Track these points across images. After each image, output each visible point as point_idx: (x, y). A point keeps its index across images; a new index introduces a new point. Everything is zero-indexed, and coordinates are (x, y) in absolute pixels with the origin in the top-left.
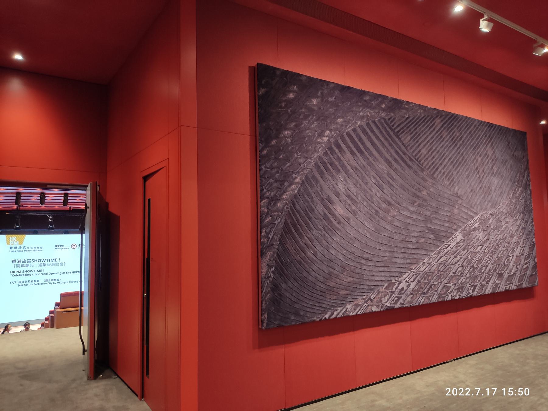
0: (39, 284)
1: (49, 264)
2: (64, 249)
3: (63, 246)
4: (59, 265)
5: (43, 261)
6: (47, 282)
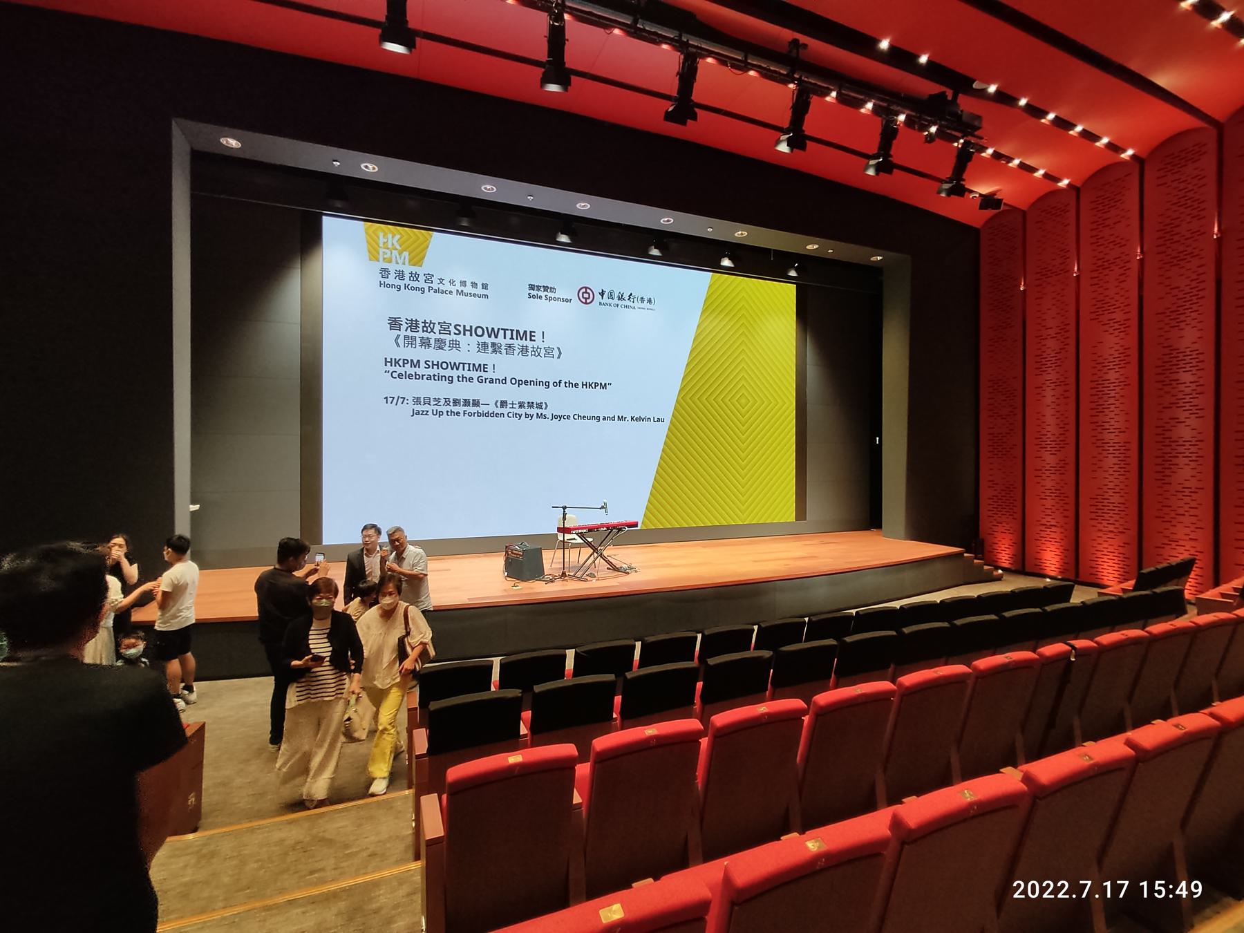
1: (510, 349)
2: (555, 299)
3: (553, 290)
5: (490, 336)
6: (503, 410)
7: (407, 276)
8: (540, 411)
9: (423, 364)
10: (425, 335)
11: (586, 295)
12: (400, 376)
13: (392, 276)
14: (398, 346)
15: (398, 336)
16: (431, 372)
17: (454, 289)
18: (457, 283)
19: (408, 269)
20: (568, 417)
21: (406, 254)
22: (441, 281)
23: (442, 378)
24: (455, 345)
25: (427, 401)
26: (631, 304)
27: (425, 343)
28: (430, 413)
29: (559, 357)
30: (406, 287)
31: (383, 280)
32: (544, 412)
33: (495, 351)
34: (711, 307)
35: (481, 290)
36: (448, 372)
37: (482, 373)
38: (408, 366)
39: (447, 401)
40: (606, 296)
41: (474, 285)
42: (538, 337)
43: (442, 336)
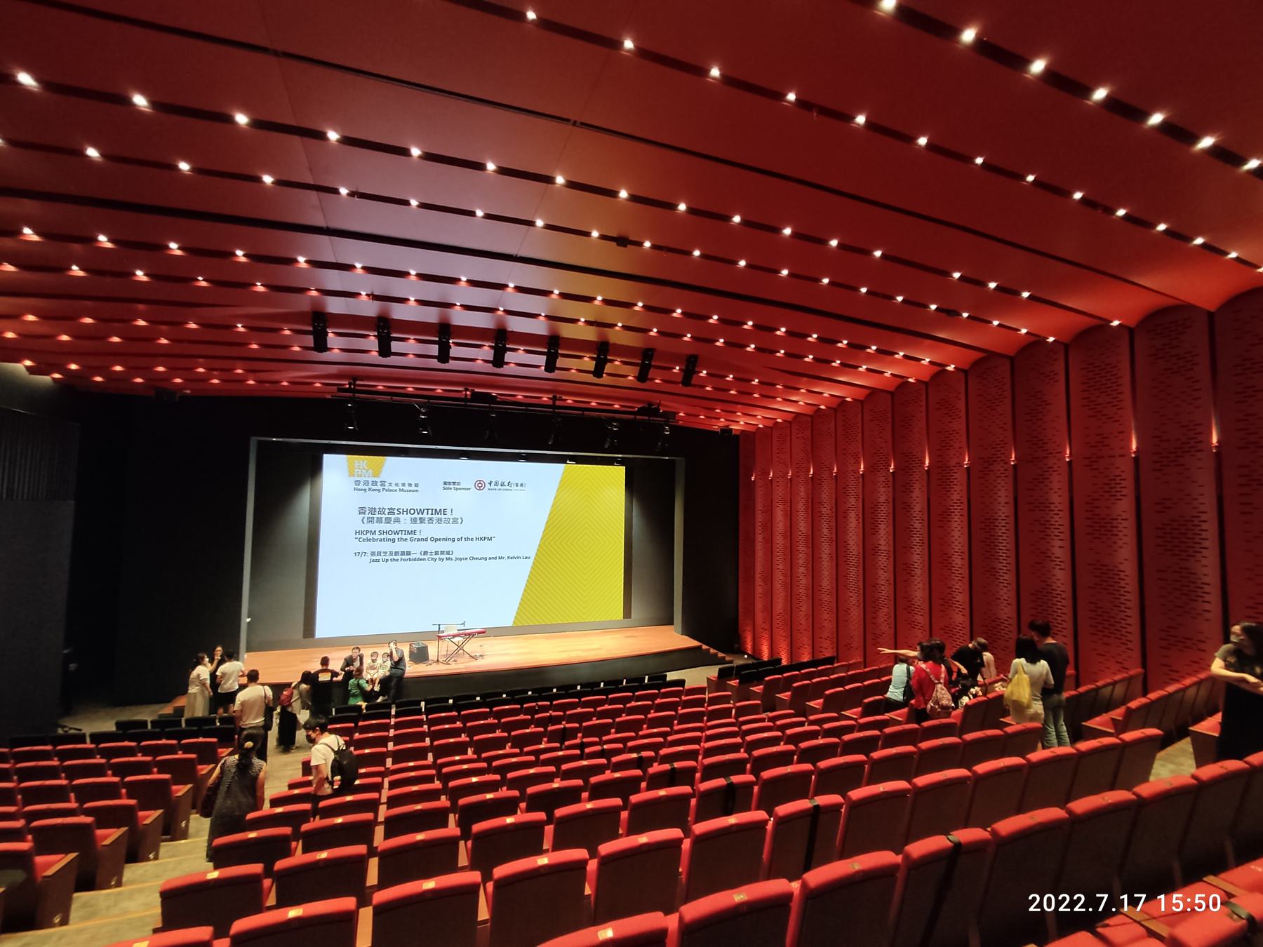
0: (410, 560)
1: (431, 520)
2: (460, 489)
3: (459, 484)
5: (418, 514)
6: (426, 557)
7: (370, 483)
8: (448, 556)
9: (377, 533)
10: (380, 516)
11: (480, 485)
14: (363, 523)
15: (364, 518)
16: (382, 537)
17: (397, 488)
18: (400, 485)
20: (466, 559)
21: (370, 471)
22: (390, 484)
24: (397, 520)
25: (379, 553)
26: (510, 488)
27: (379, 520)
28: (381, 560)
29: (461, 523)
30: (369, 489)
31: (356, 487)
32: (451, 556)
33: (421, 522)
34: (563, 485)
35: (414, 488)
36: (392, 536)
37: (413, 536)
39: (391, 553)
40: (493, 484)
42: (448, 512)
43: (390, 516)
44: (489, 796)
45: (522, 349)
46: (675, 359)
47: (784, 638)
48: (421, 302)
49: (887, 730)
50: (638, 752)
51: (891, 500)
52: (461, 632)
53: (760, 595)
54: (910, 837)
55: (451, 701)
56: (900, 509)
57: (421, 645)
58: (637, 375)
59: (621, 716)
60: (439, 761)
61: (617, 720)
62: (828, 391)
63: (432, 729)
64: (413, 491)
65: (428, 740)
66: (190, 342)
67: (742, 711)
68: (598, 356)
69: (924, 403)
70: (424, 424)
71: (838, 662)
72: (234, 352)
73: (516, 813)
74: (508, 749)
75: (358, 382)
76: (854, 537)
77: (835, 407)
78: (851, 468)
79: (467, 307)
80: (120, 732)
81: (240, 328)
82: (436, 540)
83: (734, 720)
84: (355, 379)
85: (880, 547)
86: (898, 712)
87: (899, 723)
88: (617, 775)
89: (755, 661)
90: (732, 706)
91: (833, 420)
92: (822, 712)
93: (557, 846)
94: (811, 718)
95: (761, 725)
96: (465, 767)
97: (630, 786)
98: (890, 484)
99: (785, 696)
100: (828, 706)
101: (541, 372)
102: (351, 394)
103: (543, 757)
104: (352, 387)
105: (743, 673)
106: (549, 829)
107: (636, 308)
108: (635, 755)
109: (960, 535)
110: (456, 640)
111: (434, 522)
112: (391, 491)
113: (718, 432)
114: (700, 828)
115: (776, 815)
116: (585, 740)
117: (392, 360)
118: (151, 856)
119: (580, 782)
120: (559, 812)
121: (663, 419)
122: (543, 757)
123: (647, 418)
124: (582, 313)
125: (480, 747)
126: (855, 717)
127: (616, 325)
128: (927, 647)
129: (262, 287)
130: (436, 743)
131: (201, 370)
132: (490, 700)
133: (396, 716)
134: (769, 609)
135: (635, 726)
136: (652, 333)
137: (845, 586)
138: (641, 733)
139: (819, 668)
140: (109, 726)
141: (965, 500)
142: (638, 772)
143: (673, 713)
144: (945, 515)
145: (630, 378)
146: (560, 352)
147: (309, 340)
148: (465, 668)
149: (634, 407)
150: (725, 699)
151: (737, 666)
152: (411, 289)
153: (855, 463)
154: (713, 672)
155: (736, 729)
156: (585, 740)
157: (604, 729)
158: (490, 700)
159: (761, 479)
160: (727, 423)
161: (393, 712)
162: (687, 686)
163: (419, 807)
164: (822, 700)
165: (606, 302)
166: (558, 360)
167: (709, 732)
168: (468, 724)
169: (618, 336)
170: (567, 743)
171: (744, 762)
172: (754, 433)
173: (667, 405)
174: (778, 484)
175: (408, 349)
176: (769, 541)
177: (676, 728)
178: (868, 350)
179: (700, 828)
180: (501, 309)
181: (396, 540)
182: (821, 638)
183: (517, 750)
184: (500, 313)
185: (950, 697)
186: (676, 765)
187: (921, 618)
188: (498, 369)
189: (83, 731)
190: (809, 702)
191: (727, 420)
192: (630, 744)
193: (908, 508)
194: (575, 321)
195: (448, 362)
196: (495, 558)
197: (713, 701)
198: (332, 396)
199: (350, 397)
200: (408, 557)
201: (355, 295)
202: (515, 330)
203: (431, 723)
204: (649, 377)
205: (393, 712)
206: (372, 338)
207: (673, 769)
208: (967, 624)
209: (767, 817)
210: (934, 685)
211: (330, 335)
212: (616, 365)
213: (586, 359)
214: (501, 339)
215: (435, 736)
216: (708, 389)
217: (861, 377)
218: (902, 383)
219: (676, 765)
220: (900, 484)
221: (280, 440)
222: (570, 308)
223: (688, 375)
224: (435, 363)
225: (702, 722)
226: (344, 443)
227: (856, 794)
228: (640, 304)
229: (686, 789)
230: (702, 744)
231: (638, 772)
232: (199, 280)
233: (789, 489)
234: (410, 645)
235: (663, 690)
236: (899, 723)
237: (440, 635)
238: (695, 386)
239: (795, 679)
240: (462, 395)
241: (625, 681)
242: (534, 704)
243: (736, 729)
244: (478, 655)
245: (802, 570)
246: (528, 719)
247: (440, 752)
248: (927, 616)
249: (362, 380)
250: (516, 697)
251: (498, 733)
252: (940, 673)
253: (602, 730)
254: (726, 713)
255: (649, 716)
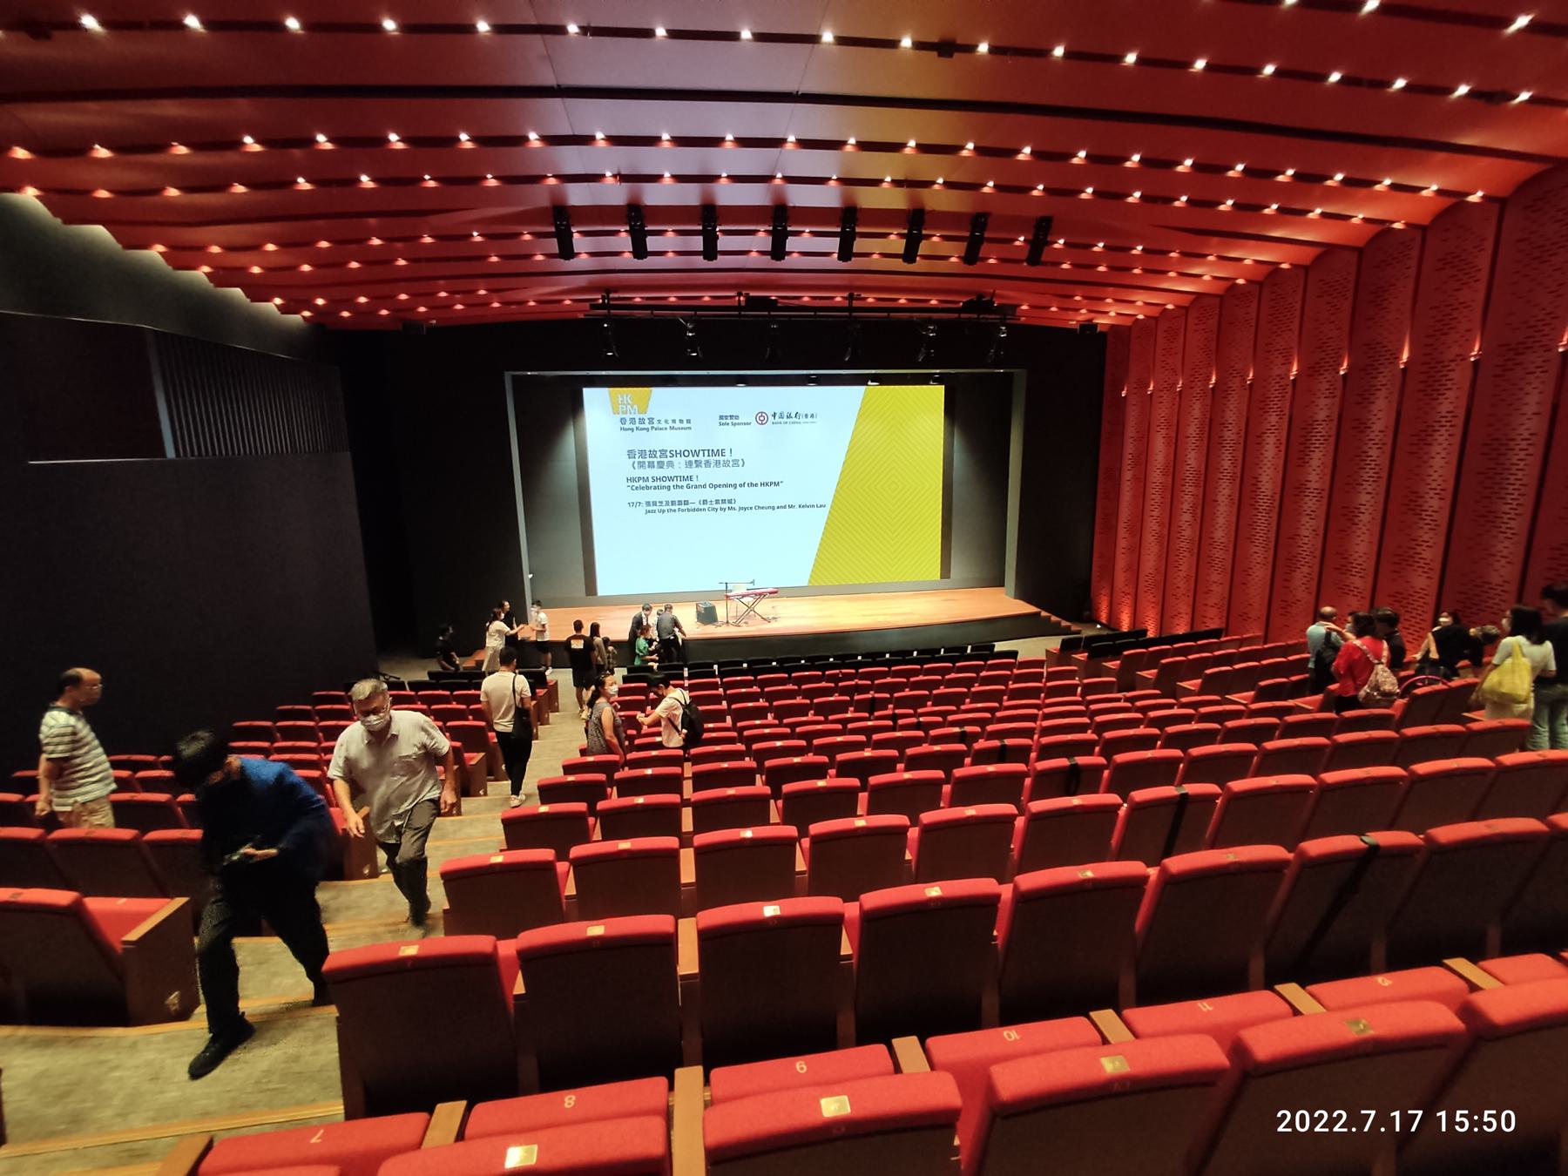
1: (708, 463)
2: (739, 424)
3: (737, 417)
4: (731, 465)
6: (706, 507)
7: (637, 421)
8: (730, 505)
9: (650, 480)
10: (651, 460)
11: (762, 418)
12: (637, 488)
13: (628, 422)
14: (634, 468)
15: (634, 462)
16: (655, 484)
17: (668, 426)
18: (670, 422)
19: (637, 417)
20: (751, 508)
21: (635, 407)
22: (659, 422)
23: (662, 487)
24: (671, 464)
25: (655, 504)
27: (651, 465)
30: (637, 428)
32: (733, 505)
33: (697, 466)
34: (863, 415)
35: (685, 424)
37: (690, 482)
38: (641, 481)
39: (667, 503)
41: (681, 421)
42: (727, 453)
43: (662, 459)
44: (797, 760)
45: (807, 230)
46: (1018, 224)
47: (1153, 605)
48: (679, 178)
49: (1290, 719)
50: (961, 727)
51: (1335, 416)
52: (750, 592)
53: (1123, 551)
54: (1307, 835)
55: (745, 665)
56: (1349, 426)
57: (708, 605)
58: (963, 255)
59: (939, 688)
60: (739, 724)
61: (935, 692)
62: (1251, 255)
63: (728, 692)
64: (685, 429)
65: (724, 703)
66: (429, 260)
67: (1088, 689)
68: (910, 231)
69: (1413, 263)
70: (692, 344)
71: (1226, 636)
72: (475, 268)
73: (826, 778)
74: (811, 716)
75: (612, 295)
76: (1269, 471)
77: (1259, 279)
78: (1276, 371)
79: (735, 179)
80: (434, 681)
81: (477, 237)
82: (716, 486)
83: (1080, 699)
84: (608, 291)
85: (1309, 485)
86: (1308, 698)
87: (1308, 711)
88: (937, 748)
89: (1110, 633)
90: (1078, 682)
91: (1256, 301)
92: (1199, 695)
93: (871, 811)
94: (1184, 700)
95: (1115, 706)
96: (767, 731)
97: (955, 759)
98: (1338, 393)
99: (1149, 674)
100: (1210, 685)
101: (833, 262)
102: (606, 311)
103: (850, 726)
104: (606, 301)
105: (1094, 645)
106: (863, 797)
107: (965, 153)
108: (957, 730)
109: (1443, 464)
110: (745, 600)
111: (712, 466)
112: (661, 429)
113: (1076, 329)
114: (1037, 806)
115: (1132, 800)
116: (897, 711)
117: (649, 262)
118: (481, 792)
119: (895, 753)
120: (873, 780)
121: (998, 317)
122: (850, 726)
123: (976, 316)
124: (886, 168)
125: (781, 713)
126: (1245, 702)
127: (934, 183)
128: (1364, 618)
129: (493, 180)
130: (733, 706)
131: (443, 294)
132: (789, 665)
133: (690, 678)
134: (1135, 569)
135: (957, 699)
136: (986, 190)
137: (1248, 538)
138: (963, 707)
139: (1199, 643)
140: (423, 676)
141: (1461, 414)
142: (962, 747)
143: (1003, 687)
144: (1423, 438)
145: (953, 260)
146: (858, 230)
147: (553, 245)
148: (759, 631)
149: (958, 302)
150: (1071, 675)
151: (1086, 637)
152: (665, 160)
153: (1283, 364)
154: (1054, 643)
155: (1083, 708)
156: (897, 711)
157: (921, 702)
158: (789, 665)
159: (1135, 394)
160: (1092, 315)
161: (686, 674)
162: (1020, 658)
163: (725, 765)
164: (1199, 681)
165: (922, 148)
166: (855, 243)
167: (1047, 710)
168: (766, 689)
169: (939, 198)
170: (876, 714)
171: (1092, 744)
172: (1130, 328)
173: (1004, 294)
174: (1161, 400)
175: (667, 242)
176: (1142, 480)
177: (1006, 704)
178: (1329, 183)
179: (1037, 806)
180: (779, 175)
181: (672, 487)
182: (1206, 605)
183: (822, 718)
184: (778, 182)
185: (1395, 681)
186: (1007, 742)
187: (1360, 582)
188: (778, 262)
189: (401, 680)
190: (1181, 682)
191: (1090, 311)
192: (950, 718)
193: (1361, 426)
194: (877, 182)
195: (716, 259)
196: (785, 507)
197: (1052, 676)
198: (585, 315)
199: (605, 315)
200: (686, 507)
201: (597, 178)
202: (797, 205)
203: (727, 686)
204: (980, 255)
205: (686, 674)
206: (624, 234)
207: (1004, 746)
208: (1433, 591)
209: (1120, 801)
210: (1371, 667)
211: (576, 236)
212: (934, 242)
213: (892, 237)
214: (780, 218)
215: (732, 699)
216: (1065, 266)
217: (1312, 229)
218: (1381, 231)
219: (1007, 742)
220: (1355, 393)
221: (536, 373)
222: (873, 164)
223: (1038, 245)
224: (700, 262)
225: (1039, 698)
226: (604, 373)
227: (1238, 785)
228: (970, 146)
229: (1021, 767)
230: (1038, 723)
231: (962, 747)
232: (425, 180)
233: (1176, 406)
234: (697, 605)
235: (989, 662)
236: (1308, 711)
237: (728, 594)
238: (1045, 264)
239: (1165, 654)
240: (734, 302)
241: (943, 650)
242: (838, 671)
243: (1083, 708)
244: (771, 617)
245: (1187, 517)
246: (831, 687)
247: (739, 715)
248: (1370, 579)
249: (616, 292)
250: (816, 663)
251: (799, 700)
252: (1382, 649)
253: (917, 702)
254: (1071, 690)
255: (973, 689)
